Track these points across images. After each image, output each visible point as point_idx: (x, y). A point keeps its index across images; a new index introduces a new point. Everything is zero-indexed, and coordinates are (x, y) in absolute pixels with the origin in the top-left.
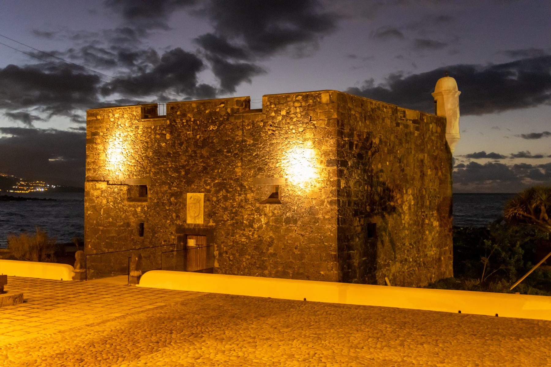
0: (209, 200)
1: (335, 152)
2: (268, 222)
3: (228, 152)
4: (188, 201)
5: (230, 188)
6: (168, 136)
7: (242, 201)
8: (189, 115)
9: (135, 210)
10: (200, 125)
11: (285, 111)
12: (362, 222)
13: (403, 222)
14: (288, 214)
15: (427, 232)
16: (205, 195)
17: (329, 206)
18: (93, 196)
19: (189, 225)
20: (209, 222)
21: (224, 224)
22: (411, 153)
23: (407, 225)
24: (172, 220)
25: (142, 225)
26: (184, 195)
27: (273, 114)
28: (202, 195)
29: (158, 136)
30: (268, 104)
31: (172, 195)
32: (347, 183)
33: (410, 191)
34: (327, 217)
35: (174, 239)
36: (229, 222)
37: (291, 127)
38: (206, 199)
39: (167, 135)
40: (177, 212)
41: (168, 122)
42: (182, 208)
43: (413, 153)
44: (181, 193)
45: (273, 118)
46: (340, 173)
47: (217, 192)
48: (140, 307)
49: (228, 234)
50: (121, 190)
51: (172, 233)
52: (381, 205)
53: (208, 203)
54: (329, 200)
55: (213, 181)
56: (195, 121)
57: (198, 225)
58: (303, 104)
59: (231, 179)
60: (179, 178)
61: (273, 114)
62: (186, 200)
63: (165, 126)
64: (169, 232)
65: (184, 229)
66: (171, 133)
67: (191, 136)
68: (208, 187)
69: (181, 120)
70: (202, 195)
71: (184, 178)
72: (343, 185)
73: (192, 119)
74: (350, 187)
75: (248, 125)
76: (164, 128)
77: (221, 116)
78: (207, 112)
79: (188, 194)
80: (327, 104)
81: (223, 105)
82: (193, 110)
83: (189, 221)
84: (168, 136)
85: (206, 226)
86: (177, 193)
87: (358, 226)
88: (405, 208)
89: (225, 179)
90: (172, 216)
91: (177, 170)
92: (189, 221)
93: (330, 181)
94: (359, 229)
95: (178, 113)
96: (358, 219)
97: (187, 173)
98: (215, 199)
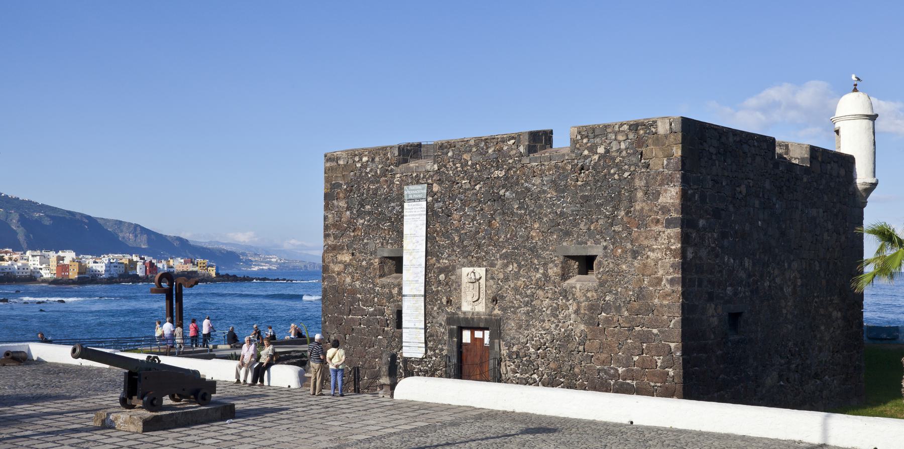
0: (493, 278)
1: (679, 208)
3: (519, 208)
4: (465, 280)
7: (540, 278)
8: (464, 156)
9: (391, 292)
10: (480, 171)
11: (603, 147)
12: (720, 310)
13: (784, 311)
14: (607, 299)
15: (823, 328)
16: (486, 271)
17: (668, 286)
18: (334, 272)
19: (464, 313)
20: (493, 309)
21: (514, 313)
22: (797, 208)
23: (790, 316)
26: (458, 271)
27: (586, 152)
28: (481, 272)
30: (579, 137)
32: (695, 253)
33: (795, 265)
34: (666, 302)
36: (524, 309)
37: (612, 171)
38: (489, 276)
39: (435, 185)
43: (800, 208)
44: (454, 268)
45: (586, 157)
46: (685, 239)
47: (506, 265)
48: (393, 427)
49: (520, 327)
50: (372, 264)
51: (441, 325)
52: (749, 286)
53: (492, 282)
54: (670, 277)
57: (478, 313)
58: (631, 136)
59: (525, 247)
61: (586, 152)
62: (460, 277)
63: (432, 173)
64: (437, 323)
66: (440, 182)
67: (468, 186)
69: (454, 165)
71: (458, 247)
72: (690, 255)
73: (470, 163)
74: (701, 258)
75: (549, 170)
78: (490, 151)
80: (666, 136)
81: (513, 141)
82: (470, 151)
83: (466, 307)
86: (447, 267)
87: (713, 316)
88: (788, 290)
89: (517, 248)
90: (441, 300)
92: (466, 307)
93: (671, 250)
94: (715, 321)
95: (450, 154)
96: (713, 306)
98: (501, 276)
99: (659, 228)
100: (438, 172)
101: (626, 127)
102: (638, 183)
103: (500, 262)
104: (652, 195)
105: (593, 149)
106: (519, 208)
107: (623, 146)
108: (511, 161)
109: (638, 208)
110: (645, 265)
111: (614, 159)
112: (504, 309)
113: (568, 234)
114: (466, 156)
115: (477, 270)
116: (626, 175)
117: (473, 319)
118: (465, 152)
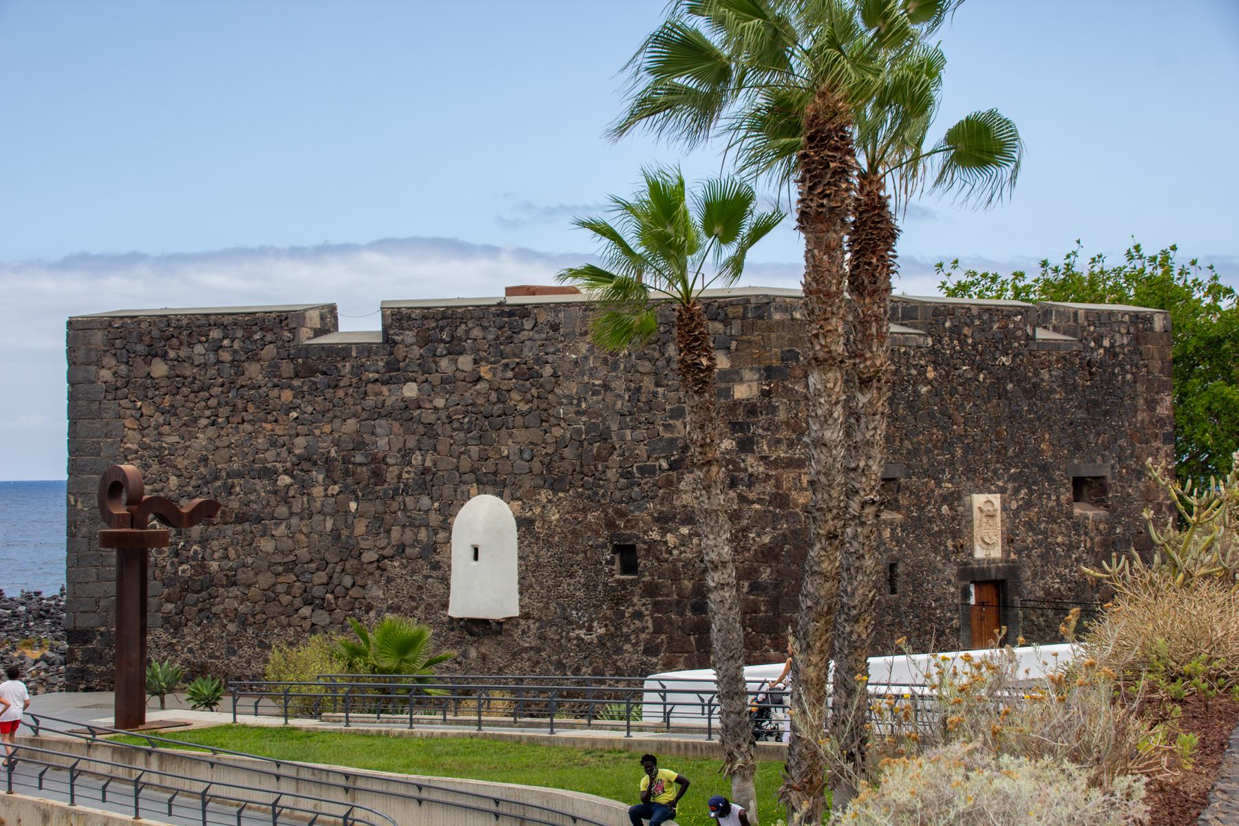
2: (1092, 547)
3: (1029, 412)
5: (1035, 483)
6: (931, 374)
7: (1052, 508)
18: (797, 506)
19: (978, 561)
21: (1028, 556)
24: (946, 557)
25: (892, 567)
28: (996, 499)
29: (914, 372)
31: (945, 499)
35: (953, 594)
39: (929, 368)
40: (955, 534)
41: (930, 341)
42: (966, 527)
44: (960, 498)
51: (949, 582)
55: (1007, 469)
56: (974, 345)
57: (994, 560)
59: (1036, 465)
60: (951, 463)
61: (1092, 344)
62: (970, 509)
64: (943, 579)
65: (972, 569)
66: (936, 365)
68: (1001, 484)
70: (996, 499)
73: (970, 341)
75: (1058, 361)
76: (923, 355)
77: (1017, 339)
79: (975, 496)
83: (979, 553)
84: (931, 374)
85: (1007, 562)
86: (952, 494)
89: (1026, 466)
91: (947, 445)
92: (979, 553)
95: (948, 324)
97: (967, 449)
99: (1157, 444)
100: (933, 351)
101: (1127, 318)
102: (1140, 388)
103: (1010, 486)
104: (1152, 404)
105: (1098, 340)
106: (1029, 412)
107: (1125, 341)
108: (1016, 345)
109: (1139, 418)
110: (1148, 489)
111: (1116, 355)
112: (1019, 553)
113: (1078, 448)
114: (966, 331)
115: (991, 497)
116: (1129, 376)
117: (989, 569)
118: (966, 324)
